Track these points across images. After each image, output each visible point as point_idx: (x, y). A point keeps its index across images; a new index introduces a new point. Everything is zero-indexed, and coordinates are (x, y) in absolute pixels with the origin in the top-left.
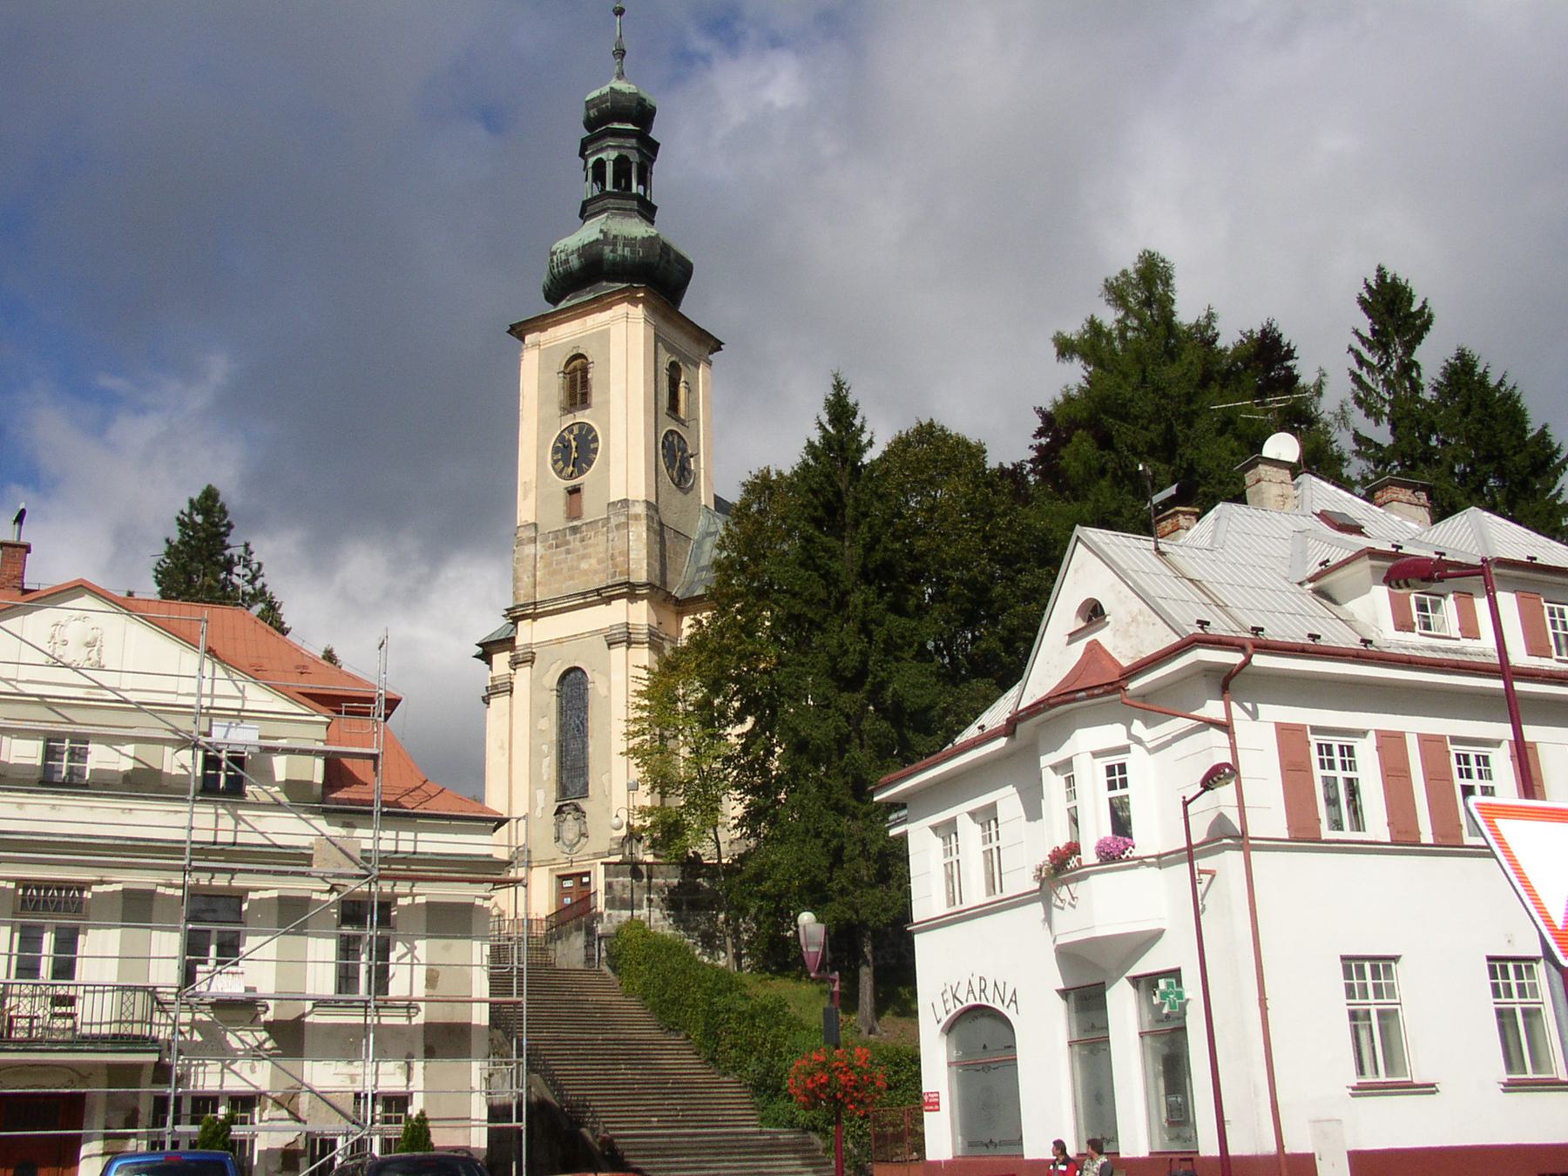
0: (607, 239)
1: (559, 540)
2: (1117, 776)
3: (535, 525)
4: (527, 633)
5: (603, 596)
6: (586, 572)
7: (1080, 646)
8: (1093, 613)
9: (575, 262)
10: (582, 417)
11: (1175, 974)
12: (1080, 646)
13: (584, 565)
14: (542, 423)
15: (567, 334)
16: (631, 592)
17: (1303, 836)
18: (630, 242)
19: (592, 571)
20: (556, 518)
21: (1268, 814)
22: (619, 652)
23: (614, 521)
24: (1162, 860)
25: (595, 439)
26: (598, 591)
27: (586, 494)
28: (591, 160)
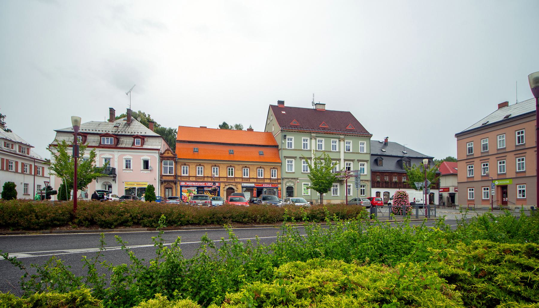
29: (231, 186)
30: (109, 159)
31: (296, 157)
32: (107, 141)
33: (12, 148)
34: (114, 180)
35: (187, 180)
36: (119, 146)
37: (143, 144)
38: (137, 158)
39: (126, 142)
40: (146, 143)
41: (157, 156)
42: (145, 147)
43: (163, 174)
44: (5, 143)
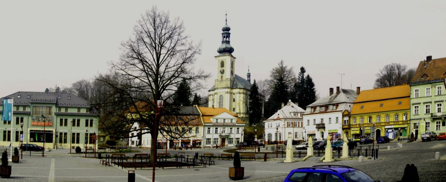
0: (226, 48)
1: (220, 81)
3: (218, 80)
4: (216, 91)
5: (225, 88)
8: (279, 115)
9: (222, 50)
10: (223, 68)
13: (223, 85)
16: (228, 88)
17: (288, 127)
21: (286, 126)
23: (227, 80)
26: (225, 88)
27: (223, 76)
28: (223, 36)
29: (378, 128)
31: (420, 103)
32: (323, 109)
33: (298, 115)
34: (324, 130)
35: (355, 126)
36: (328, 111)
37: (337, 108)
38: (333, 116)
39: (331, 107)
40: (338, 107)
41: (341, 114)
42: (338, 110)
43: (344, 125)
44: (294, 114)
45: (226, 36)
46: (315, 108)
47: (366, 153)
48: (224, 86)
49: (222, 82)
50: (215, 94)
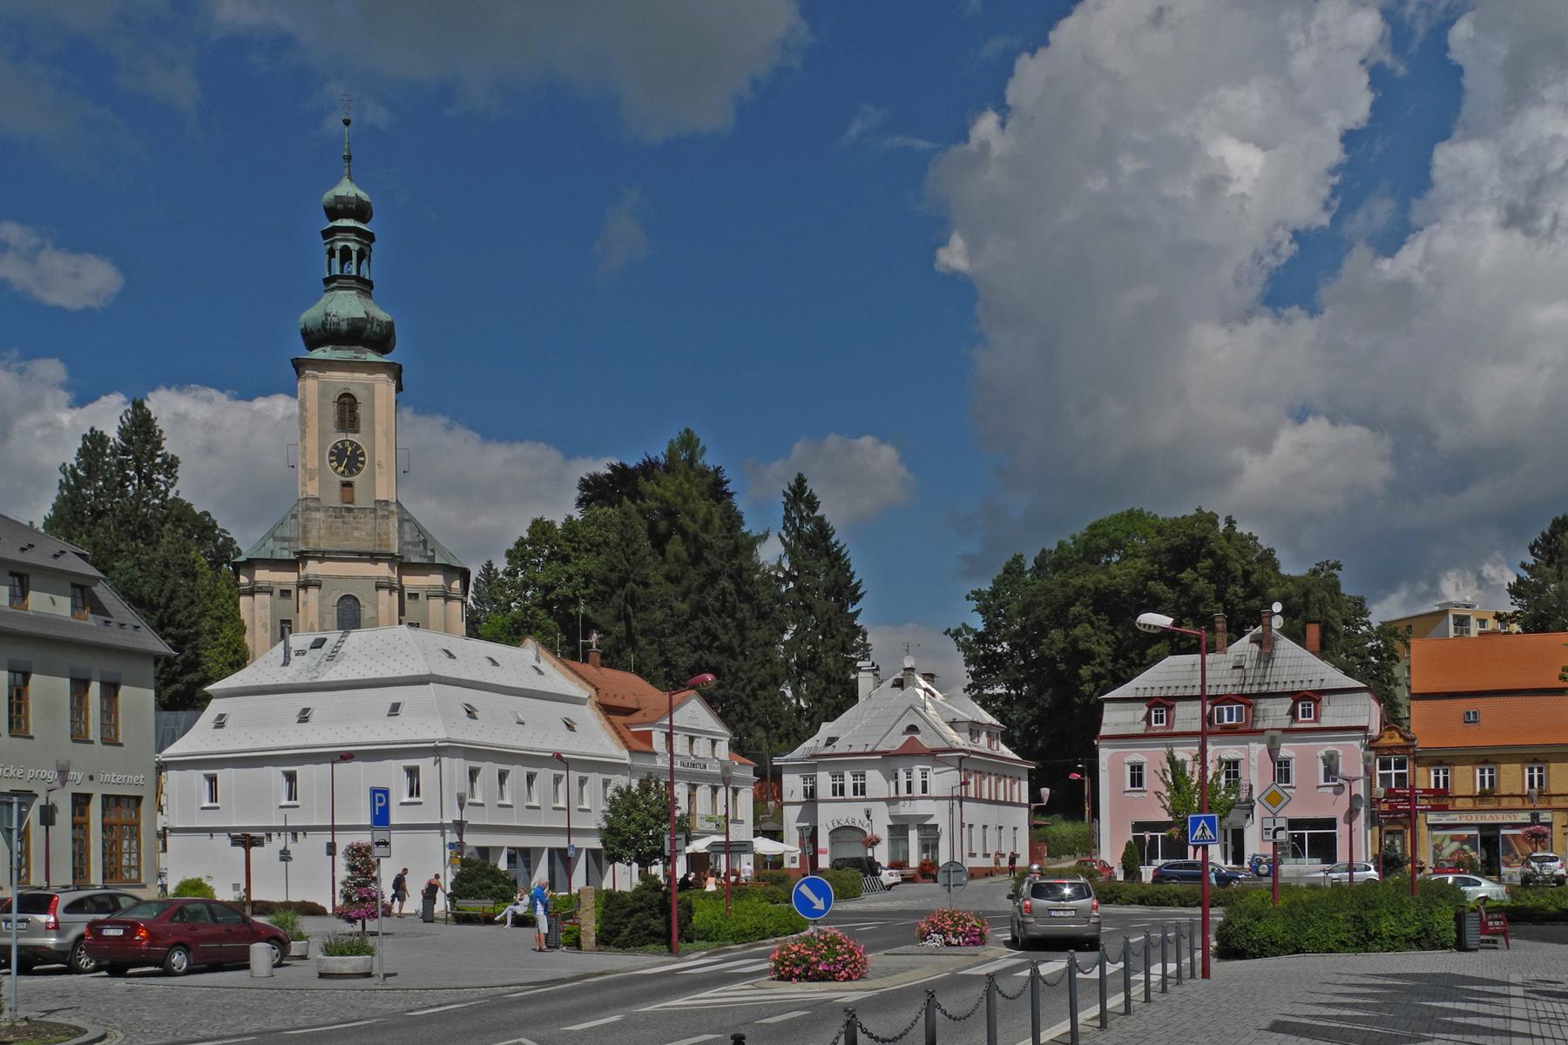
0: (368, 319)
1: (338, 513)
2: (924, 775)
4: (313, 568)
5: (374, 557)
6: (357, 539)
7: (907, 737)
9: (344, 326)
10: (351, 437)
11: (936, 826)
12: (907, 737)
13: (356, 534)
14: (322, 433)
15: (340, 378)
18: (380, 323)
19: (361, 538)
20: (334, 498)
22: (384, 593)
23: (380, 513)
24: (936, 798)
25: (362, 455)
26: (372, 555)
27: (356, 485)
30: (1236, 763)
45: (354, 247)
46: (1161, 704)
47: (1460, 930)
48: (364, 547)
49: (349, 518)
50: (305, 585)
